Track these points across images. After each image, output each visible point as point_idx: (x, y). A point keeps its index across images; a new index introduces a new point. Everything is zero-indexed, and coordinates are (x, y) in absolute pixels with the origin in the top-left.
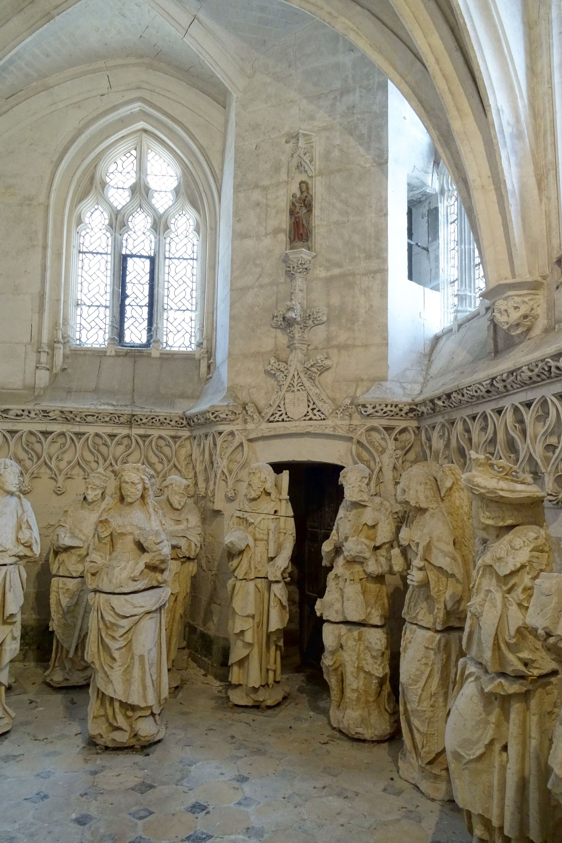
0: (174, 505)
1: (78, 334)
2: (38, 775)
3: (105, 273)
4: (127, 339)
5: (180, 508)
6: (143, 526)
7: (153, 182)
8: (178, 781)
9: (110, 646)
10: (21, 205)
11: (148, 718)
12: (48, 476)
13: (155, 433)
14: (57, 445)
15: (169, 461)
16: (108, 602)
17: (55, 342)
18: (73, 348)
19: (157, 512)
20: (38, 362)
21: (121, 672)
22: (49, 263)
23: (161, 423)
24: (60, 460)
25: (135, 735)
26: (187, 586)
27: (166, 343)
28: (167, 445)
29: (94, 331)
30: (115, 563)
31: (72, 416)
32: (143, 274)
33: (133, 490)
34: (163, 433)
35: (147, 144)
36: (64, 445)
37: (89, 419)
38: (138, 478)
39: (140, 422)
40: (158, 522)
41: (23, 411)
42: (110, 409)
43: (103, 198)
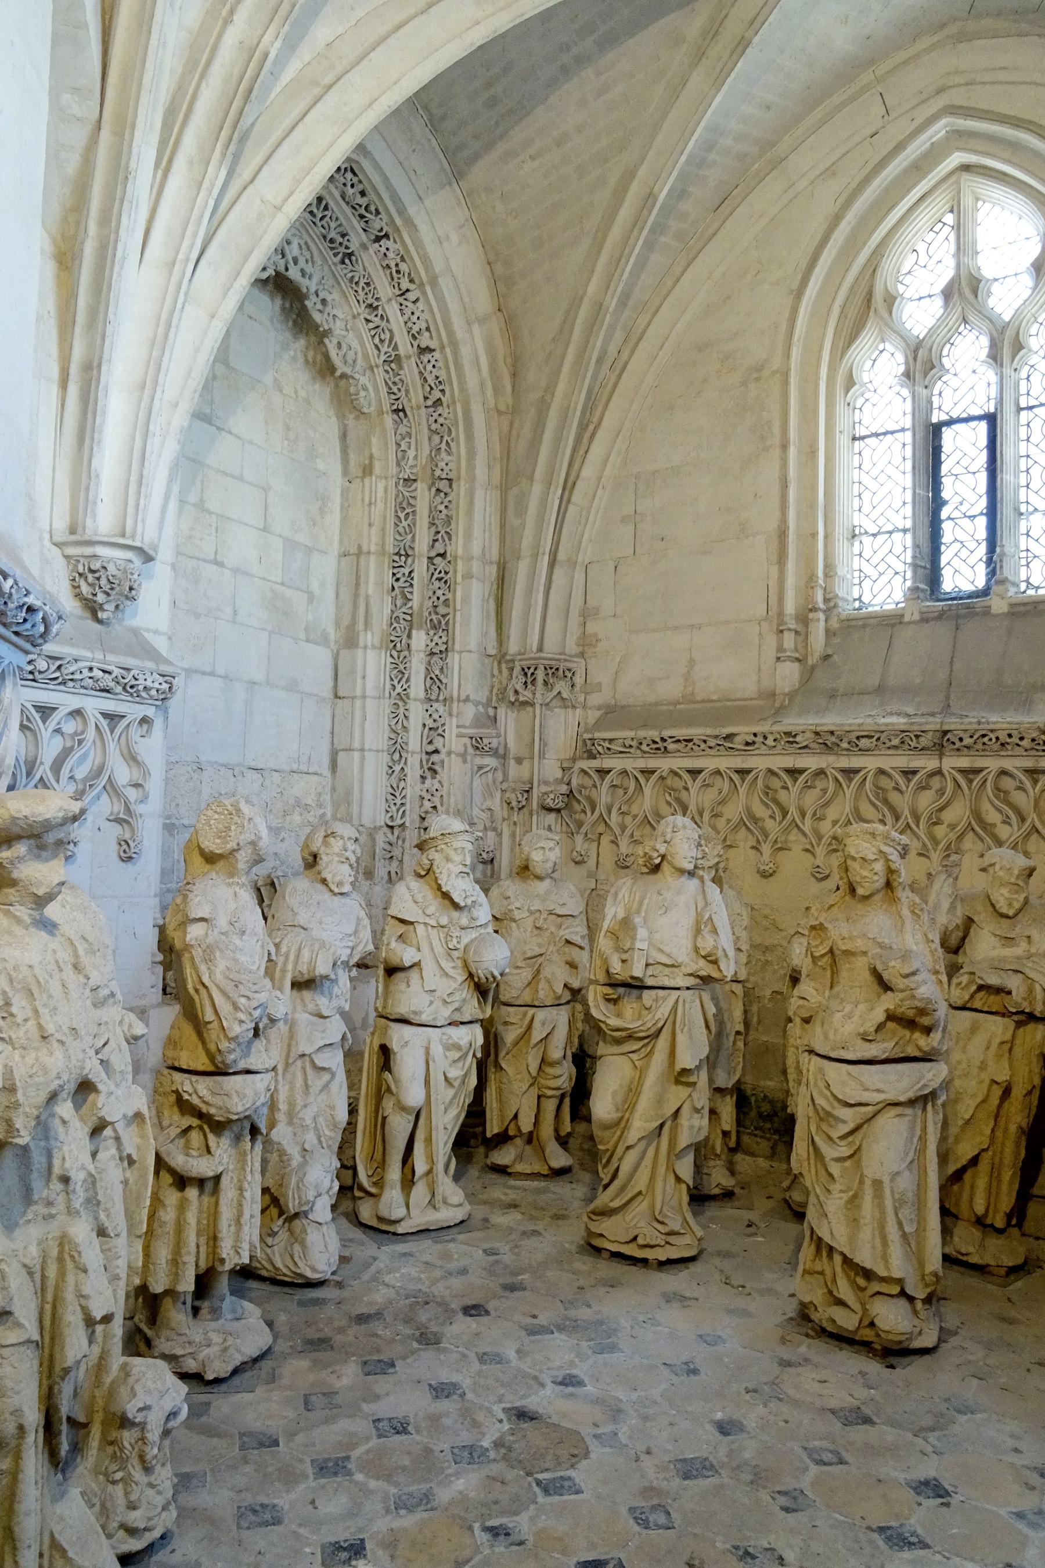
0: (997, 907)
1: (856, 589)
2: (701, 1336)
3: (901, 468)
4: (947, 585)
5: (1011, 913)
6: (886, 941)
7: (987, 266)
8: (922, 1429)
9: (823, 1150)
10: (744, 384)
11: (895, 1300)
12: (801, 847)
13: (992, 764)
14: (815, 793)
15: (1023, 819)
16: (821, 1071)
17: (811, 610)
18: (842, 617)
19: (919, 916)
20: (780, 649)
21: (843, 1202)
22: (792, 474)
23: (1002, 744)
24: (820, 819)
25: (872, 1324)
26: (1031, 1071)
27: (1027, 581)
28: (1019, 788)
29: (884, 579)
30: (834, 1004)
31: (833, 739)
32: (973, 452)
33: (865, 873)
34: (1008, 764)
35: (973, 192)
36: (824, 791)
37: (864, 743)
38: (874, 850)
39: (958, 744)
40: (919, 936)
41: (755, 735)
42: (900, 721)
43: (891, 328)
